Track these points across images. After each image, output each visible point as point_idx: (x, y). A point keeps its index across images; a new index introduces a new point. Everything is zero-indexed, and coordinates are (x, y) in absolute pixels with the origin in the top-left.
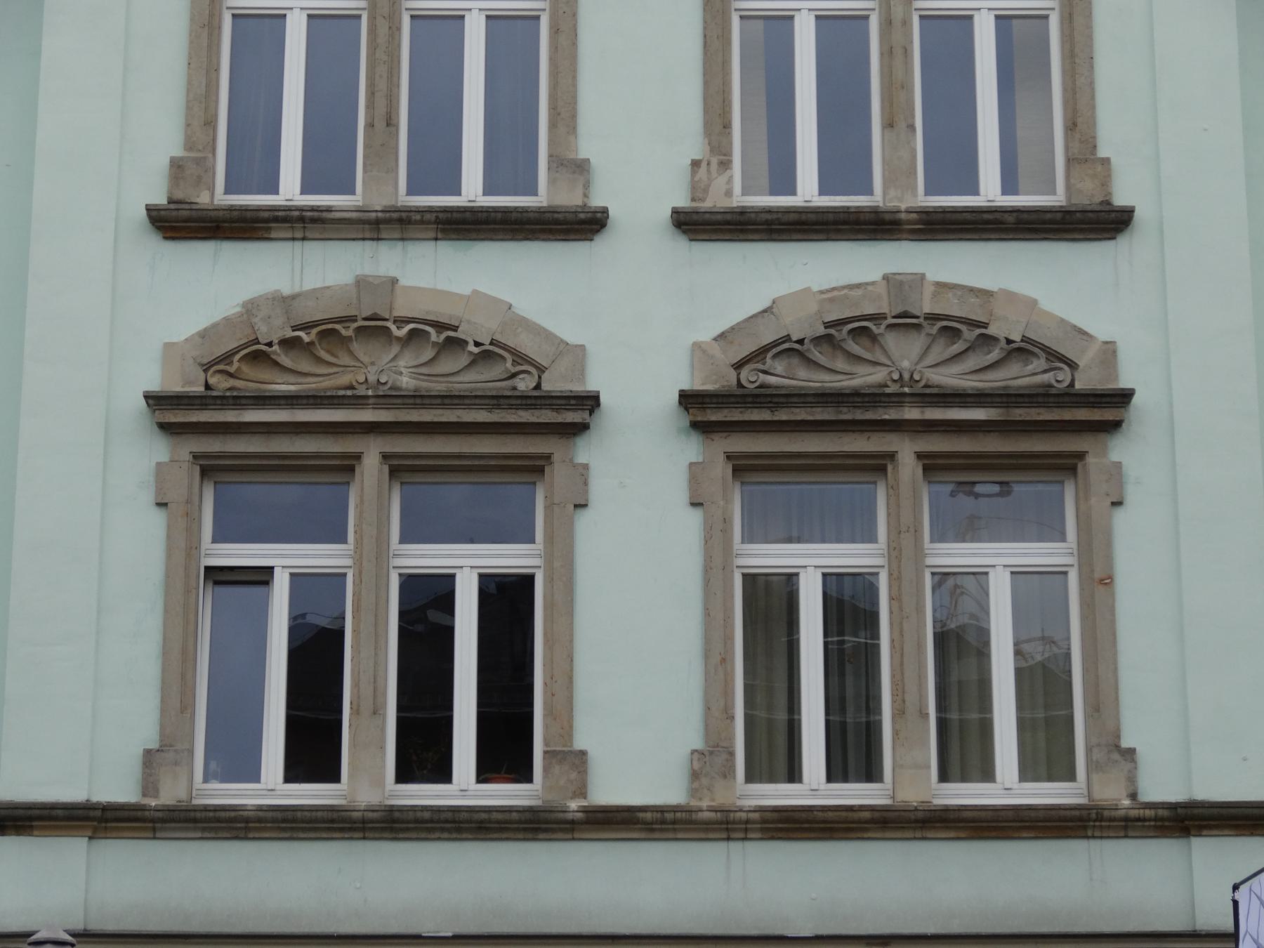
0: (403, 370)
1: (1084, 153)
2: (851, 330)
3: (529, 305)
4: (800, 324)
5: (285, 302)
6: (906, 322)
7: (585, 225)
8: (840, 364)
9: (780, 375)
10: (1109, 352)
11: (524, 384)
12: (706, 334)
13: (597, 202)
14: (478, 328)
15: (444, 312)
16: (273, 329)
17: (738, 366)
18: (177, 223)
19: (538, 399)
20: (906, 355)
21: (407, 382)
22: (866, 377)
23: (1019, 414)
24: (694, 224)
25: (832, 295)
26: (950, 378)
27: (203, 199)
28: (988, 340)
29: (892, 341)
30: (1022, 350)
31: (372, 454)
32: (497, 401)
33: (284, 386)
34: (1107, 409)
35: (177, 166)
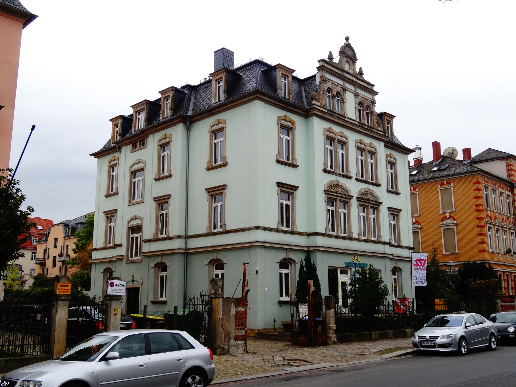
0: (339, 190)
1: (377, 179)
7: (350, 178)
20: (369, 196)
21: (340, 192)
22: (367, 198)
24: (357, 180)
26: (371, 199)
31: (339, 198)
32: (345, 195)
33: (332, 191)
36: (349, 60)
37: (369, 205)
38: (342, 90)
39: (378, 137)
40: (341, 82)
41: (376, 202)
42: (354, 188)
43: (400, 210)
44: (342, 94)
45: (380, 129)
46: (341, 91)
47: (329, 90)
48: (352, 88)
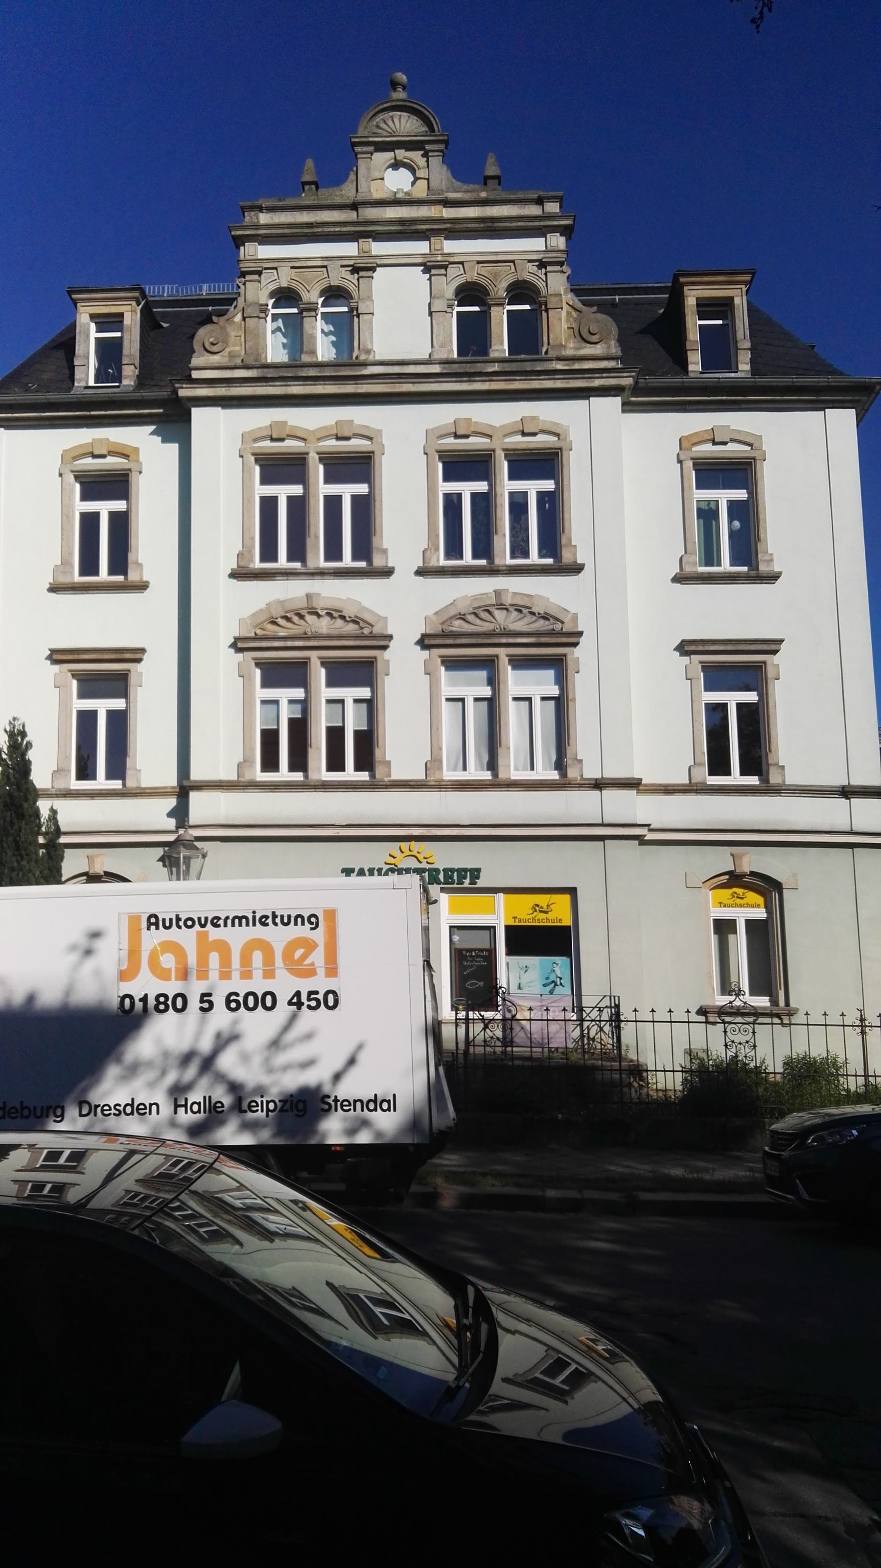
0: (324, 625)
2: (482, 610)
3: (367, 603)
4: (463, 608)
5: (281, 603)
6: (502, 607)
7: (388, 572)
8: (478, 622)
9: (458, 626)
10: (575, 617)
11: (366, 631)
12: (430, 612)
13: (390, 565)
14: (349, 612)
15: (337, 605)
16: (277, 612)
17: (442, 623)
18: (240, 574)
19: (372, 636)
21: (324, 631)
22: (486, 627)
23: (543, 640)
25: (475, 598)
27: (251, 566)
28: (533, 613)
29: (497, 613)
30: (545, 617)
32: (357, 637)
34: (573, 638)
35: (240, 555)
36: (401, 154)
37: (502, 652)
38: (348, 276)
39: (559, 384)
40: (349, 249)
41: (552, 633)
42: (404, 603)
43: (772, 646)
44: (352, 288)
45: (597, 350)
46: (349, 281)
47: (286, 296)
48: (421, 247)
